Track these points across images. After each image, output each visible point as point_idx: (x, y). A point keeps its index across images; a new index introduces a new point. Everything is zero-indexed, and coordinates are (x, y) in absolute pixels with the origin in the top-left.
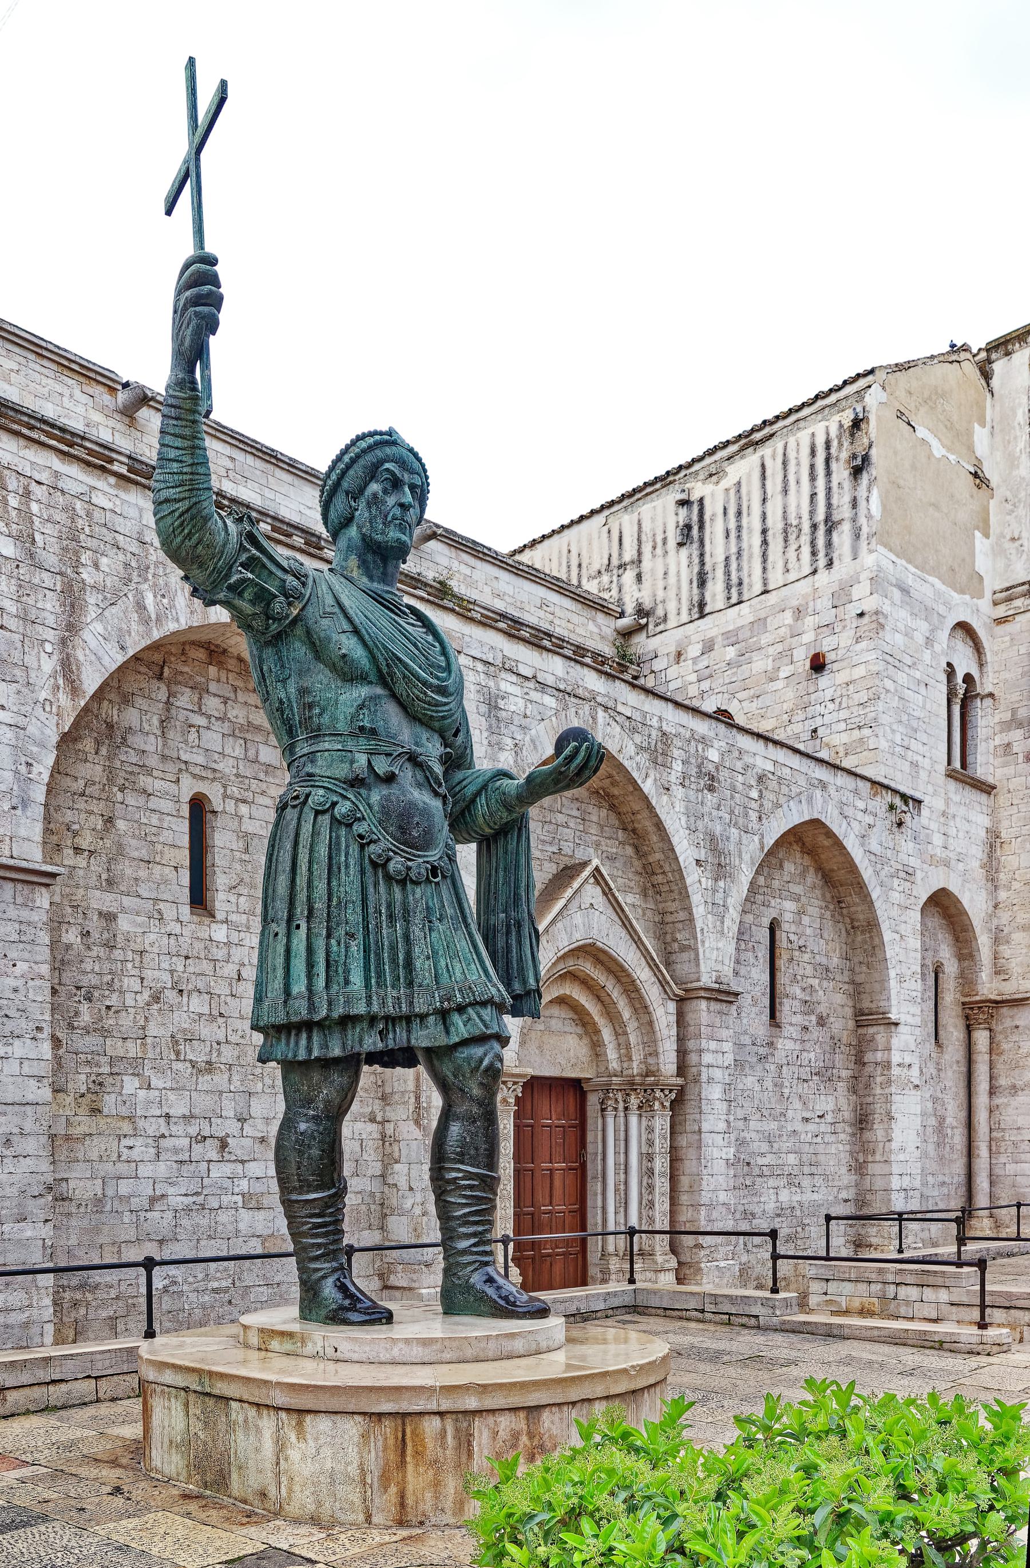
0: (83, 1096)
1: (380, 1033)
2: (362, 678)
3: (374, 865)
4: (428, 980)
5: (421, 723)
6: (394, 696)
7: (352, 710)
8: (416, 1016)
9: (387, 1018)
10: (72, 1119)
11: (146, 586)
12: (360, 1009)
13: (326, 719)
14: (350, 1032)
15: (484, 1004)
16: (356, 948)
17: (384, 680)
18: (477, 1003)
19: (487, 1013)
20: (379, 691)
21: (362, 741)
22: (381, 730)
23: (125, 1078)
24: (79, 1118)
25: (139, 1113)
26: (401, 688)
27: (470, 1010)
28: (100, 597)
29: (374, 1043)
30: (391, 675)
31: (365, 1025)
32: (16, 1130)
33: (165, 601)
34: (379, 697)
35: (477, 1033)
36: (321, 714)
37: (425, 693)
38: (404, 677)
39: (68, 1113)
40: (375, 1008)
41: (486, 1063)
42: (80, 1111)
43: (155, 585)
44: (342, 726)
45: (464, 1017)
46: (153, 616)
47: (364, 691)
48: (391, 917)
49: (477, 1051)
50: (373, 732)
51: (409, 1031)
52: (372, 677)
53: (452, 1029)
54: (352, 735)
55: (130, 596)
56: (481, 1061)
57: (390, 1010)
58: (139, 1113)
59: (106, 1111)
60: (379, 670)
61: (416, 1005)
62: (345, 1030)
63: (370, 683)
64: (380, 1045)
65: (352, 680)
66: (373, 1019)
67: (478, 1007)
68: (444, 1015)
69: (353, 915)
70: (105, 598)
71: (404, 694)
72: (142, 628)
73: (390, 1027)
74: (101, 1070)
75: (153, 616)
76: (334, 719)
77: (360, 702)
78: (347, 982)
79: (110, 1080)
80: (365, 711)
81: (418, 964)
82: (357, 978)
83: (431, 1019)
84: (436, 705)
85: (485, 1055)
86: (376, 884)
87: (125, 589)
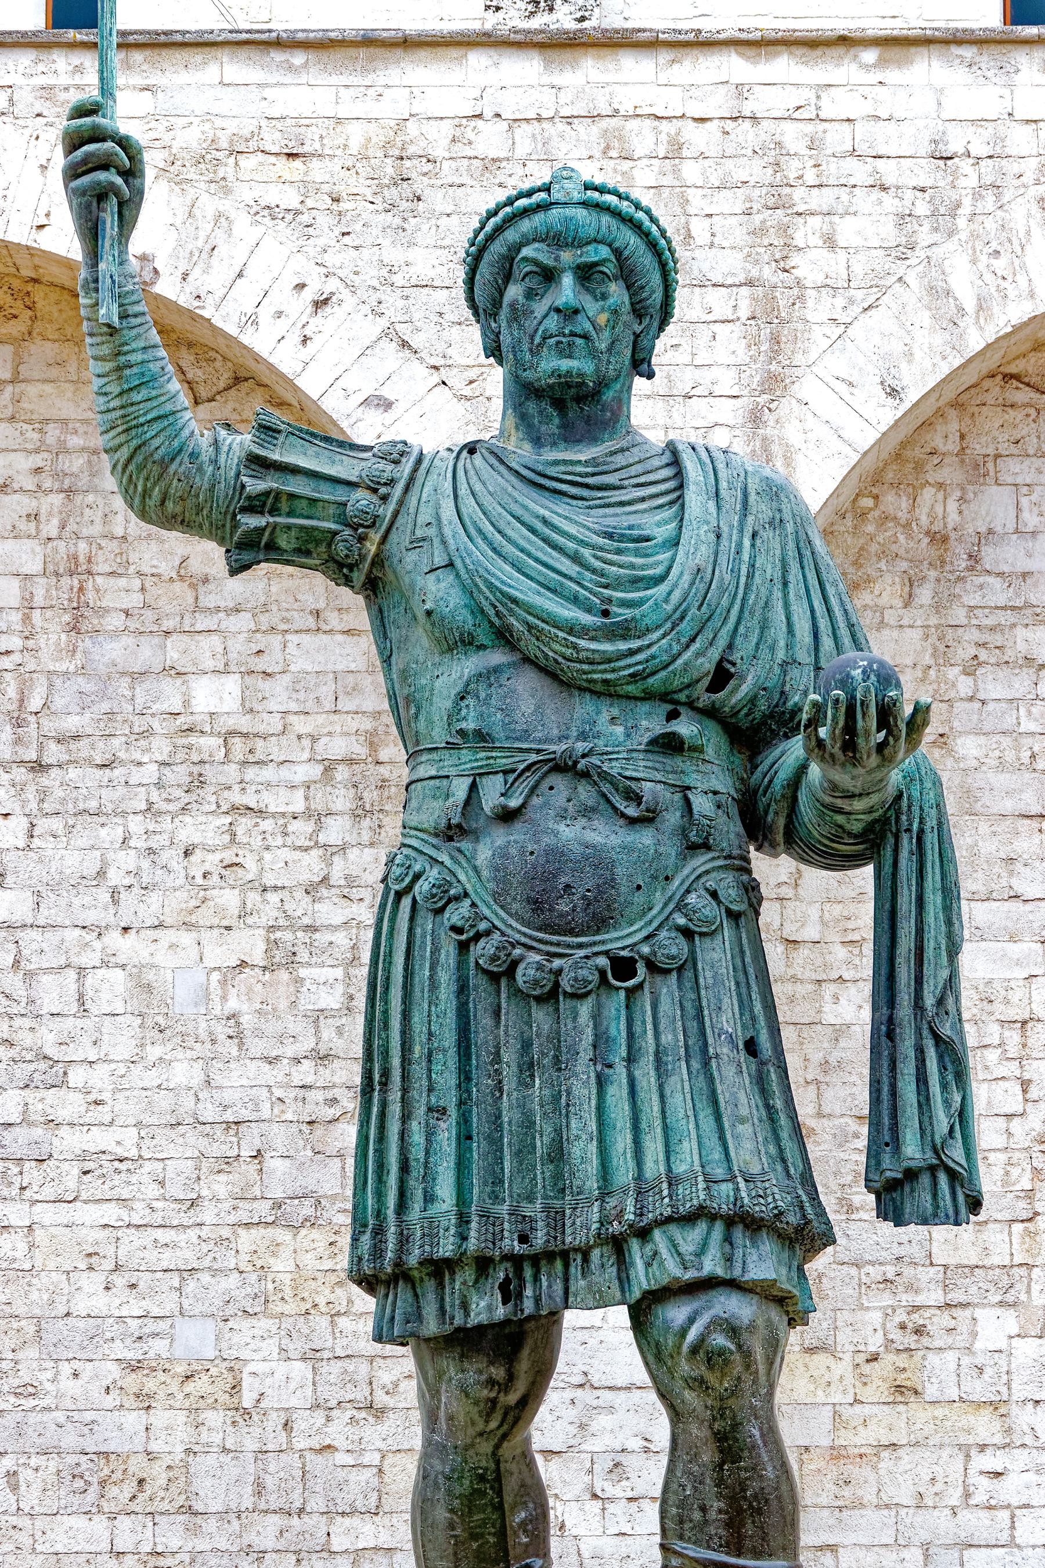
0: (874, 1358)
1: (504, 1287)
2: (467, 643)
3: (494, 978)
4: (593, 1185)
5: (598, 694)
6: (527, 660)
7: (448, 704)
8: (576, 1250)
9: (516, 1261)
10: (847, 1412)
11: (951, 245)
12: (446, 1248)
13: (422, 725)
14: (447, 1291)
15: (690, 1219)
16: (446, 1133)
17: (504, 637)
18: (669, 1220)
19: (689, 1239)
20: (497, 657)
21: (466, 755)
22: (498, 732)
23: (979, 1313)
24: (867, 1410)
25: (1018, 1394)
26: (531, 646)
27: (657, 1234)
28: (840, 301)
29: (490, 1308)
30: (509, 628)
31: (467, 1274)
32: (636, 1444)
33: (1000, 264)
34: (496, 670)
35: (665, 1281)
36: (416, 716)
37: (575, 647)
38: (530, 627)
39: (837, 1398)
40: (472, 1244)
41: (692, 1335)
42: (868, 1394)
43: (974, 236)
44: (439, 735)
45: (648, 1249)
46: (970, 306)
47: (469, 665)
48: (528, 1068)
49: (677, 1313)
50: (481, 737)
51: (566, 1280)
52: (483, 638)
53: (632, 1273)
54: (451, 746)
55: (911, 278)
56: (683, 1332)
57: (511, 1244)
58: (1018, 1394)
59: (931, 1392)
60: (492, 624)
61: (568, 1231)
62: (441, 1285)
63: (482, 647)
64: (501, 1312)
65: (450, 650)
66: (483, 1264)
67: (673, 1229)
68: (618, 1245)
69: (447, 1078)
70: (851, 301)
71: (539, 654)
72: (939, 339)
73: (528, 1273)
74: (920, 1300)
75: (970, 306)
76: (430, 722)
77: (460, 687)
78: (429, 1198)
79: (944, 1320)
80: (470, 701)
81: (576, 1151)
82: (445, 1190)
83: (596, 1254)
84: (610, 661)
85: (691, 1320)
86: (497, 1013)
87: (900, 269)
